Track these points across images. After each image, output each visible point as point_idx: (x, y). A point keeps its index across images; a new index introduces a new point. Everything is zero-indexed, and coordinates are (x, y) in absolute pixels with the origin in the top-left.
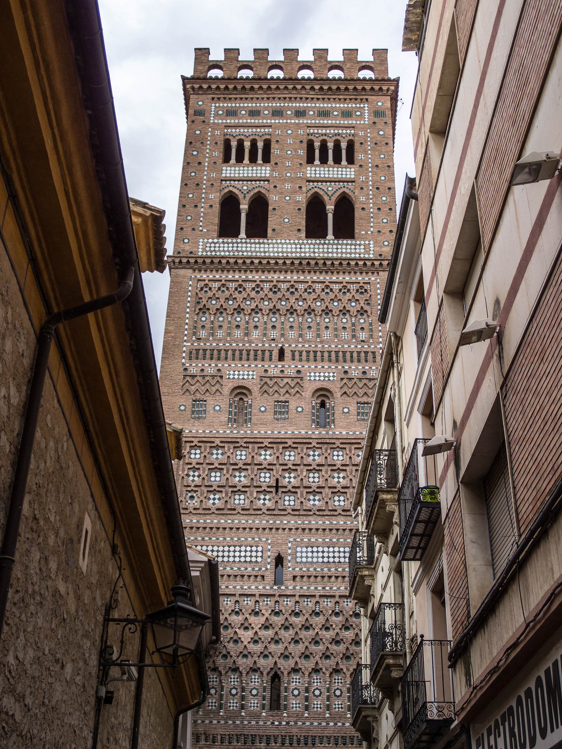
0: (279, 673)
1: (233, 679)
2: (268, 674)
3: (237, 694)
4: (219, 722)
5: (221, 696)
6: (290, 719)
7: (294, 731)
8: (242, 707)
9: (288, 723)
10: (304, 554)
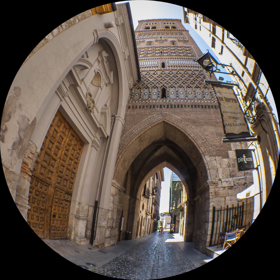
0: (165, 88)
1: (146, 91)
2: (160, 88)
3: (147, 94)
4: (139, 102)
5: (141, 95)
6: (170, 100)
7: (173, 103)
8: (149, 97)
9: (169, 101)
10: (171, 62)
